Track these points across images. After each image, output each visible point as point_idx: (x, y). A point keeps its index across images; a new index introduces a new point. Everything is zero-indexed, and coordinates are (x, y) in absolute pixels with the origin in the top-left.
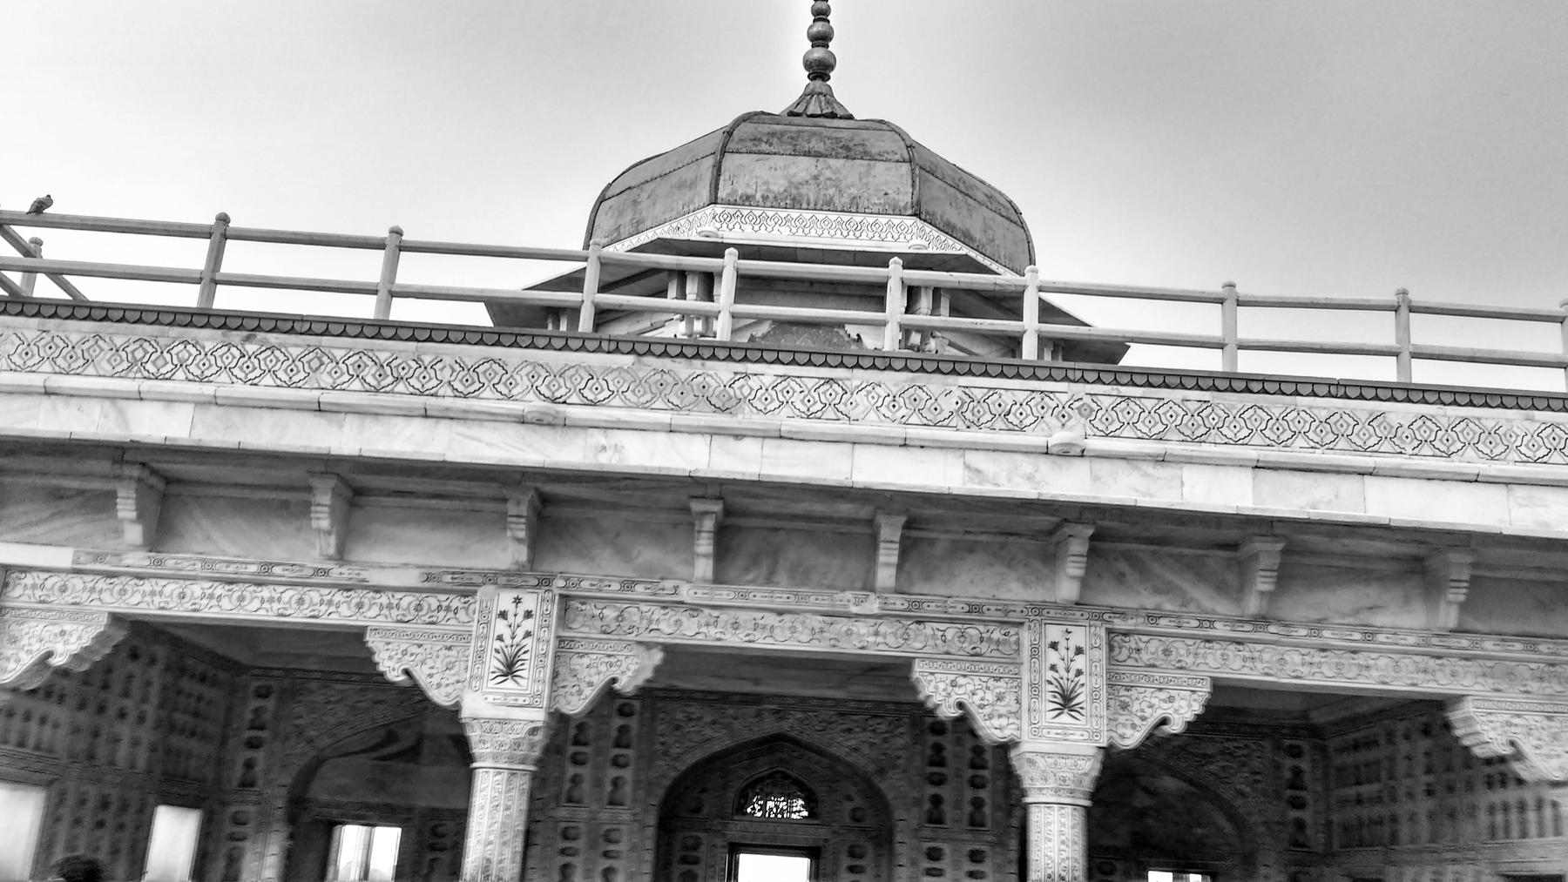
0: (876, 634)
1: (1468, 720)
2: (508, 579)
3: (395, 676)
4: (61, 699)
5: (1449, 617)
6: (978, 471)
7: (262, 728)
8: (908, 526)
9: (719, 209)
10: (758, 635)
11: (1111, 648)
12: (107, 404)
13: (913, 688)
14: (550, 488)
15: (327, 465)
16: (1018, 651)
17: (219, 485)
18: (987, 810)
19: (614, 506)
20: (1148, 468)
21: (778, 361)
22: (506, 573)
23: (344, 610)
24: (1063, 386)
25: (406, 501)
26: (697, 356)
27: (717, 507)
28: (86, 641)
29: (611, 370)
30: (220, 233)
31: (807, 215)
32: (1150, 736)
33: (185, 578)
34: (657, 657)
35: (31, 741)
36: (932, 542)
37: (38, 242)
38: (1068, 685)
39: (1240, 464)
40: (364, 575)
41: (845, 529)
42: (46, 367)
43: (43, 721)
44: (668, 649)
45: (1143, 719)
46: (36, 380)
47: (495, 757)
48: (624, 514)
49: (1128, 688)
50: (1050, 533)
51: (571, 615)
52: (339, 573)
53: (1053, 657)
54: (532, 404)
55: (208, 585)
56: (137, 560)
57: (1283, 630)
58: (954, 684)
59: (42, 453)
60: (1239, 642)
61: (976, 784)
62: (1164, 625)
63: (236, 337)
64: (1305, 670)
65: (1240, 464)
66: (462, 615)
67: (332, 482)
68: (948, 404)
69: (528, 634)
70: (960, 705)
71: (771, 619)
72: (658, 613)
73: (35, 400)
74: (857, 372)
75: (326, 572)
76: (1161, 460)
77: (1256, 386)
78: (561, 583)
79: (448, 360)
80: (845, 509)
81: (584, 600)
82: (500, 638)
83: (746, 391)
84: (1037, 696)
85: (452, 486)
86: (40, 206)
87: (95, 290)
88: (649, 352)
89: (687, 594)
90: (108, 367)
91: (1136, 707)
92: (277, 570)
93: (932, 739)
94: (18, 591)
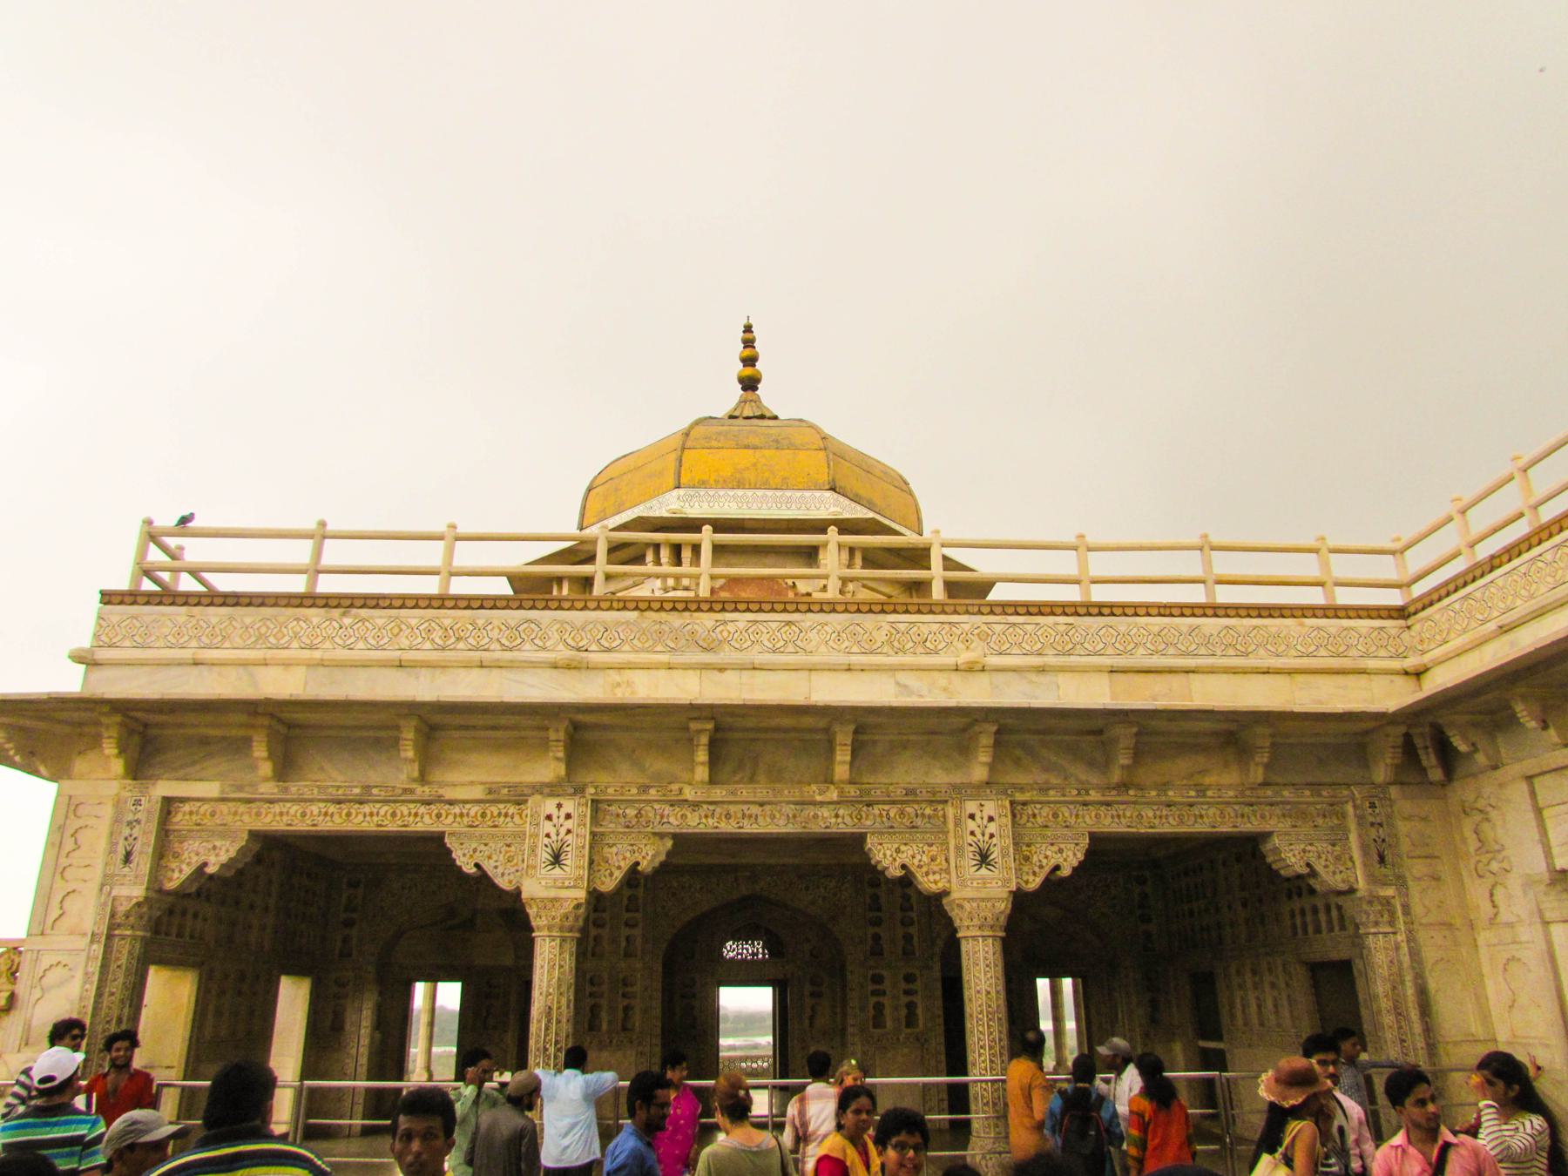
0: (837, 816)
1: (1276, 850)
2: (550, 789)
3: (469, 869)
4: (208, 898)
5: (1258, 774)
6: (905, 686)
7: (354, 910)
8: (856, 732)
9: (681, 492)
10: (746, 822)
11: (1014, 816)
12: (241, 670)
13: (866, 856)
14: (581, 717)
15: (411, 709)
16: (945, 822)
17: (330, 727)
18: (916, 939)
19: (627, 729)
20: (1033, 677)
21: (748, 610)
22: (549, 785)
23: (427, 819)
24: (965, 618)
25: (472, 733)
26: (686, 609)
27: (710, 726)
28: (233, 854)
29: (618, 624)
30: (321, 535)
31: (749, 493)
32: (1047, 880)
33: (305, 801)
34: (669, 843)
35: (187, 932)
36: (875, 742)
37: (181, 548)
38: (984, 846)
39: (1099, 670)
40: (441, 792)
41: (808, 736)
42: (194, 643)
43: (195, 916)
44: (675, 836)
45: (1041, 867)
46: (187, 654)
47: (550, 928)
48: (637, 734)
49: (1028, 845)
50: (964, 730)
51: (600, 815)
52: (423, 791)
53: (971, 825)
54: (563, 654)
55: (322, 805)
56: (269, 789)
57: (1140, 793)
58: (898, 851)
59: (194, 710)
60: (1108, 804)
61: (906, 923)
62: (1053, 795)
63: (337, 612)
64: (1157, 821)
65: (1099, 670)
66: (517, 819)
67: (414, 722)
68: (880, 637)
69: (569, 831)
70: (904, 867)
71: (755, 810)
72: (667, 810)
73: (188, 669)
74: (810, 615)
75: (412, 791)
76: (1042, 670)
77: (1106, 611)
78: (592, 790)
79: (496, 623)
80: (808, 721)
81: (610, 803)
82: (548, 836)
83: (725, 634)
84: (962, 856)
85: (503, 721)
86: (184, 520)
87: (224, 583)
88: (649, 608)
89: (689, 794)
90: (238, 640)
91: (1035, 859)
92: (375, 791)
93: (869, 891)
94: (179, 817)
